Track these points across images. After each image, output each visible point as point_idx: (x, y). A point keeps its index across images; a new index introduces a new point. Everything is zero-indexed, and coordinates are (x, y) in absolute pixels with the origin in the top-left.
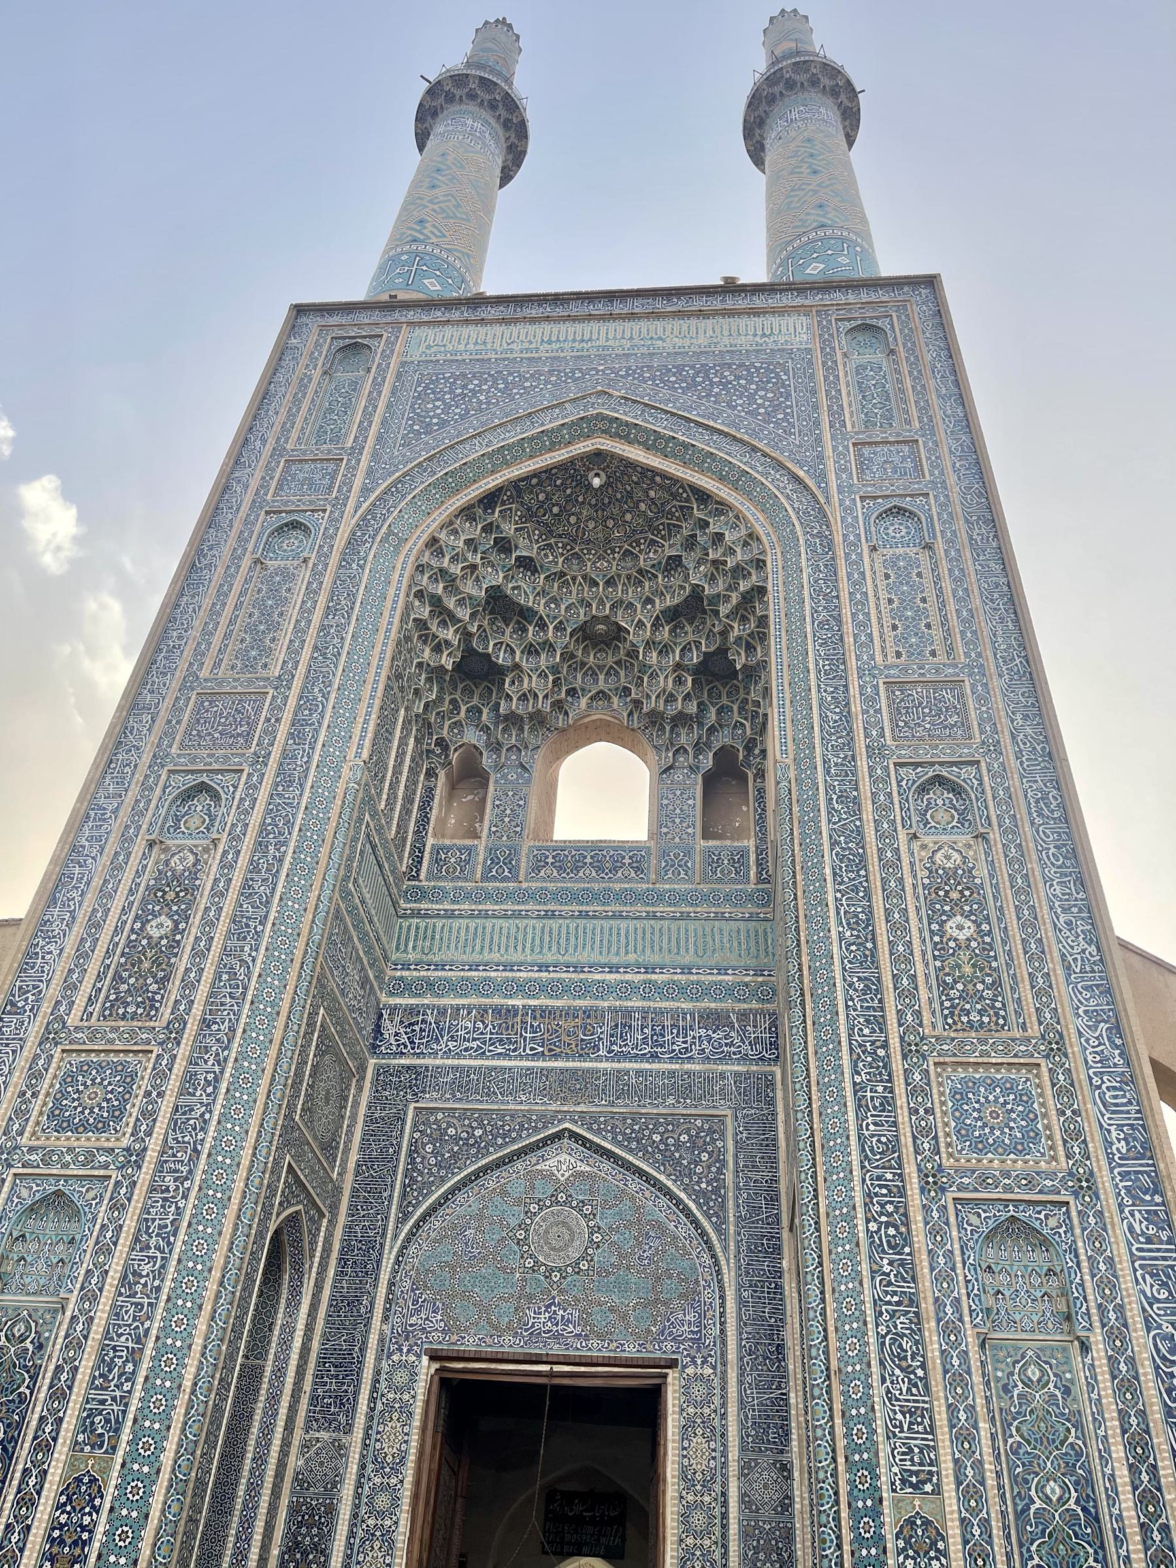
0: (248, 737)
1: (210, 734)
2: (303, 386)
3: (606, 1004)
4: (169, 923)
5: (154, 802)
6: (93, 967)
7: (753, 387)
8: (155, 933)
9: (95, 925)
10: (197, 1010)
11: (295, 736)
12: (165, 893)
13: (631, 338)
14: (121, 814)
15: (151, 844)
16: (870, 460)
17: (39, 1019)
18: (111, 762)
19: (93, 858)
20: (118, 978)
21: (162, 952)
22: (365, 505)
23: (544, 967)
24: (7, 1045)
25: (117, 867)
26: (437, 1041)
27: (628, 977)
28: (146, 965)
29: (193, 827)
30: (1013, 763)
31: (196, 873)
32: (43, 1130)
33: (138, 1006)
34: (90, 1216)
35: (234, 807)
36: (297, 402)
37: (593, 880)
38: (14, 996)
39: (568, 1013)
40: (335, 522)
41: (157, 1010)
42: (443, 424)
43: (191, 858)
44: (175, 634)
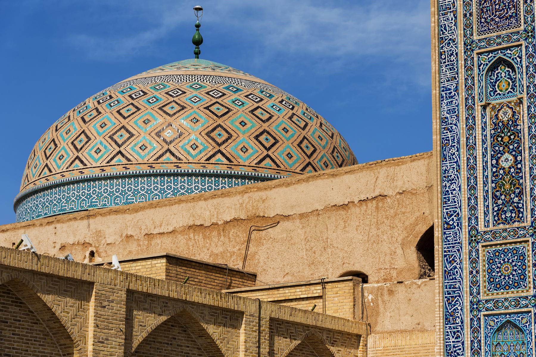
0: (516, 15)
1: (492, 20)
4: (511, 158)
5: (476, 78)
6: (480, 194)
8: (506, 165)
9: (472, 168)
12: (502, 138)
14: (460, 92)
15: (484, 107)
17: (463, 230)
18: (441, 55)
19: (455, 125)
20: (495, 197)
21: (513, 177)
24: (453, 247)
25: (471, 128)
28: (507, 186)
29: (504, 89)
31: (516, 122)
32: (489, 290)
33: (512, 213)
34: (528, 332)
35: (525, 74)
38: (445, 218)
41: (522, 213)
43: (510, 112)
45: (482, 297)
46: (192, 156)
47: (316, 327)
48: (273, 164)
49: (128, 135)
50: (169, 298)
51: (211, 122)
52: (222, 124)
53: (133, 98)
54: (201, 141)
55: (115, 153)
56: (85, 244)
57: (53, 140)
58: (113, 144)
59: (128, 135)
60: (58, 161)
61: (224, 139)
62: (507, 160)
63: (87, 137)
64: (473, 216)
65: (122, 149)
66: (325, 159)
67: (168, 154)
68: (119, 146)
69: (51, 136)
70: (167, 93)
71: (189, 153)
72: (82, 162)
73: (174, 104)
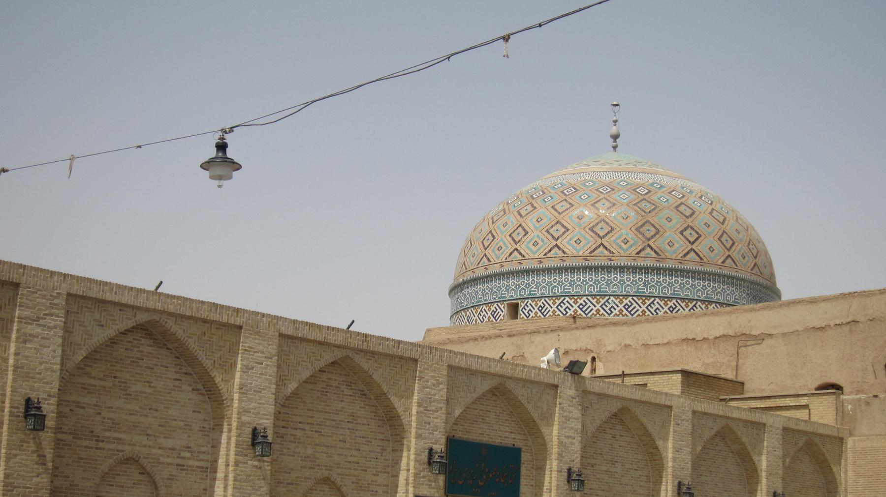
46: (623, 250)
47: (812, 433)
49: (563, 230)
50: (718, 416)
51: (640, 218)
52: (650, 220)
54: (631, 236)
56: (587, 351)
57: (491, 232)
58: (550, 237)
59: (563, 230)
60: (497, 252)
63: (524, 230)
65: (558, 242)
66: (742, 251)
67: (602, 247)
68: (556, 240)
69: (487, 227)
70: (597, 190)
71: (620, 247)
72: (520, 253)
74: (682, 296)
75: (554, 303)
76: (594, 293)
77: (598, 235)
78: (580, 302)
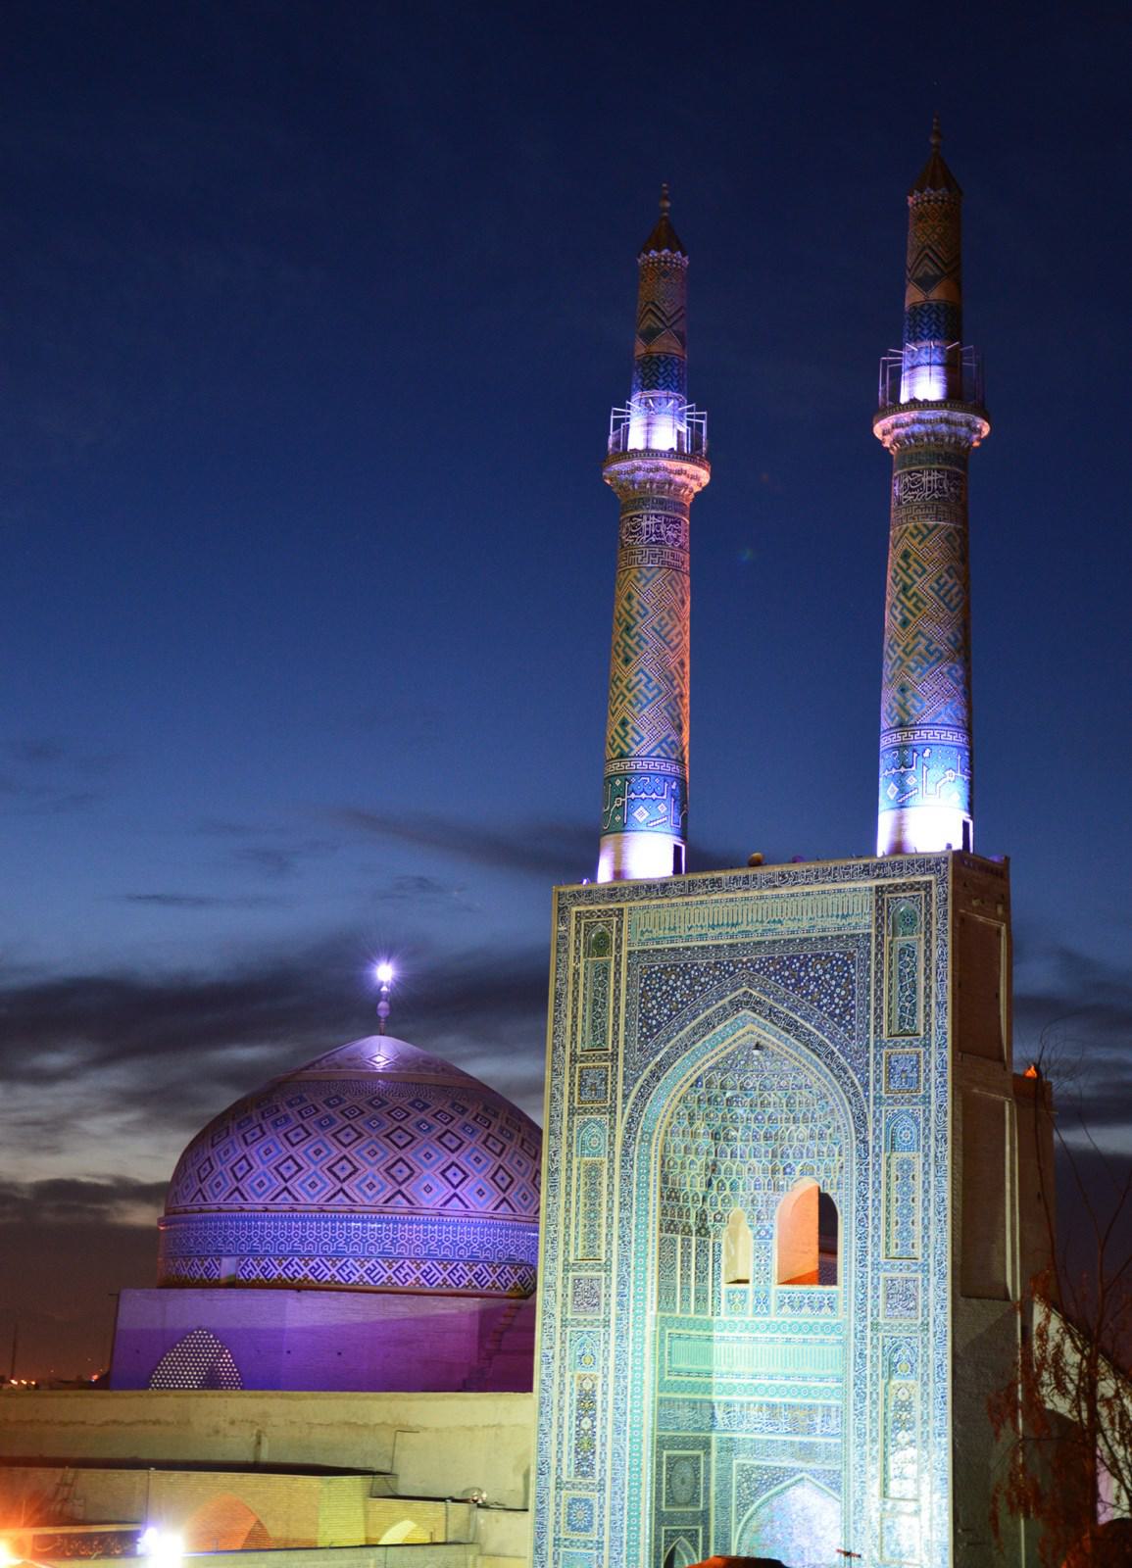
2: (576, 982)
3: (818, 1402)
4: (589, 1422)
6: (565, 1449)
7: (834, 983)
10: (608, 1473)
11: (620, 1304)
13: (762, 922)
16: (894, 1068)
20: (576, 1452)
22: (627, 1111)
23: (788, 1378)
26: (741, 1422)
27: (828, 1385)
30: (932, 1340)
36: (575, 1000)
37: (809, 1316)
39: (800, 1407)
40: (612, 1128)
42: (659, 1025)
44: (552, 1228)
45: (562, 1536)
48: (460, 1204)
49: (295, 1168)
53: (303, 1118)
55: (280, 1188)
59: (295, 1168)
61: (405, 1175)
62: (586, 1423)
64: (559, 1467)
67: (341, 1195)
68: (286, 1181)
71: (365, 1193)
73: (349, 1130)
74: (440, 1256)
75: (280, 1264)
76: (329, 1253)
77: (338, 1178)
78: (312, 1264)
